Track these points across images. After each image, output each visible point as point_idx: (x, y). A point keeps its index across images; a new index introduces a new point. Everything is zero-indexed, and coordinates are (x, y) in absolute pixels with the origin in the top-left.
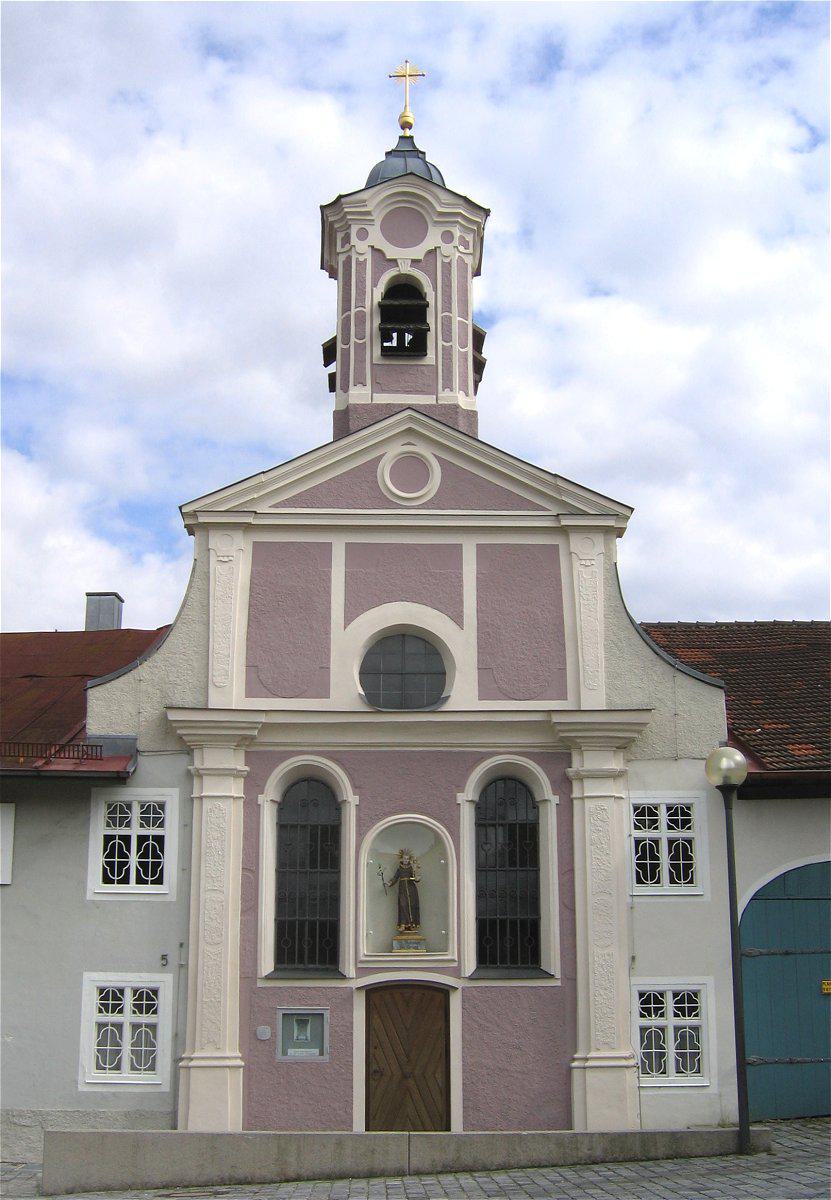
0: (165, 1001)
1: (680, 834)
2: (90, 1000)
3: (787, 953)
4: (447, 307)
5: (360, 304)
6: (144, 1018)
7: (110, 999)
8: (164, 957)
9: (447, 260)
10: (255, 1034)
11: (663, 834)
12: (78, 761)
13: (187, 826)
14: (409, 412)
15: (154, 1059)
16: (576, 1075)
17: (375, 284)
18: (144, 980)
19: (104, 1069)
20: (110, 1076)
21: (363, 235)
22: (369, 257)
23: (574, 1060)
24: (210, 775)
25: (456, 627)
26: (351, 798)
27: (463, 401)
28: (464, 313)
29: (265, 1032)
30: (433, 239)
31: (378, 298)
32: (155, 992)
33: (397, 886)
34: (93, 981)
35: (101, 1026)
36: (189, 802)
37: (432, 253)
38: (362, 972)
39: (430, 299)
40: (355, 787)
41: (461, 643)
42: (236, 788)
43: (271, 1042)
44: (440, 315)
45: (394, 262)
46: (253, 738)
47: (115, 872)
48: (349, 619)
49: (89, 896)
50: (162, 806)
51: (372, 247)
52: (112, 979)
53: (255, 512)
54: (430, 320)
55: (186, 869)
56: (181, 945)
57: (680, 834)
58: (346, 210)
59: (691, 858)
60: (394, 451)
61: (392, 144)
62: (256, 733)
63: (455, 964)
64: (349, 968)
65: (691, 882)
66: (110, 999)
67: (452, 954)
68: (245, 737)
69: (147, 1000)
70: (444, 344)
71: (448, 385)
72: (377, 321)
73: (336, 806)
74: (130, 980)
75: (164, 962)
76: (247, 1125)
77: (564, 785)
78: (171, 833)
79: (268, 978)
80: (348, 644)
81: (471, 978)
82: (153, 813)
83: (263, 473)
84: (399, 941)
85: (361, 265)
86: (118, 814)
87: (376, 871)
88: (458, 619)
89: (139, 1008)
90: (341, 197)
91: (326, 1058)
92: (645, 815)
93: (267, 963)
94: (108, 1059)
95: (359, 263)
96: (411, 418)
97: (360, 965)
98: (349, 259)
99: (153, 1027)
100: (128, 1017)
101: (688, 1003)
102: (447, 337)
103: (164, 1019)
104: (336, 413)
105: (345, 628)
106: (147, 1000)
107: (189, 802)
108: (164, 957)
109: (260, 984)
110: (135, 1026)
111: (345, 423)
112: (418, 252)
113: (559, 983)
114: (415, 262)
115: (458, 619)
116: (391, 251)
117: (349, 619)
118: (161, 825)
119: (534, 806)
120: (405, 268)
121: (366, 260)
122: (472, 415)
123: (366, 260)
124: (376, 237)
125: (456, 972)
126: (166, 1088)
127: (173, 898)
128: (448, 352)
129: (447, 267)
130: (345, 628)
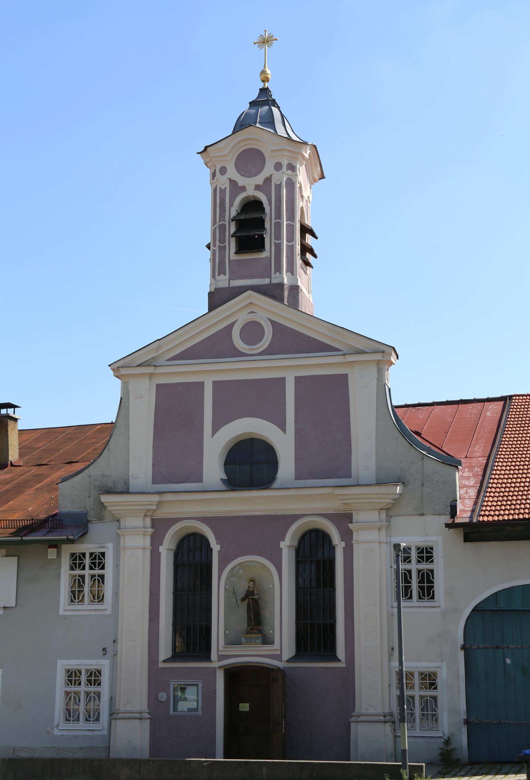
0: (105, 678)
1: (425, 566)
2: (61, 677)
3: (498, 647)
4: (279, 215)
5: (222, 219)
6: (93, 689)
7: (72, 677)
8: (104, 649)
9: (278, 183)
10: (157, 698)
11: (414, 567)
12: (49, 530)
13: (117, 566)
14: (249, 292)
15: (99, 713)
16: (353, 726)
17: (231, 205)
18: (92, 664)
19: (70, 720)
20: (72, 726)
21: (223, 171)
22: (227, 185)
23: (353, 716)
24: (128, 535)
25: (282, 432)
26: (215, 547)
27: (286, 280)
28: (291, 217)
29: (162, 697)
30: (268, 170)
31: (234, 213)
32: (100, 672)
33: (246, 602)
34: (62, 665)
35: (67, 693)
36: (117, 553)
37: (268, 180)
38: (221, 658)
39: (267, 210)
40: (218, 539)
41: (284, 445)
42: (148, 541)
43: (167, 702)
44: (273, 221)
45: (243, 189)
46: (154, 510)
47: (76, 596)
48: (215, 431)
49: (61, 612)
50: (103, 554)
51: (230, 179)
52: (73, 664)
53: (155, 366)
54: (267, 225)
55: (116, 594)
56: (114, 642)
57: (425, 566)
58: (211, 155)
59: (432, 582)
60: (242, 319)
61: (254, 95)
62: (154, 507)
63: (279, 653)
64: (214, 656)
65: (433, 598)
66: (72, 677)
67: (277, 645)
68: (148, 510)
69: (94, 678)
70: (280, 239)
71: (279, 269)
72: (233, 229)
73: (210, 551)
74: (85, 664)
75: (104, 652)
76: (150, 756)
77: (347, 536)
78: (109, 572)
79: (164, 661)
80: (214, 446)
81: (287, 661)
82: (98, 561)
83: (159, 340)
84: (246, 638)
85: (223, 191)
86: (77, 561)
87: (231, 592)
88: (283, 427)
89: (89, 681)
90: (206, 148)
91: (200, 713)
92: (402, 554)
93: (165, 650)
94: (70, 715)
95: (223, 191)
96: (250, 296)
97: (220, 654)
98: (216, 186)
99: (99, 694)
100: (83, 689)
101: (430, 680)
102: (278, 236)
103: (105, 689)
104: (210, 294)
105: (212, 436)
106: (94, 678)
107: (117, 553)
108: (104, 649)
109: (161, 665)
110: (87, 694)
111: (217, 299)
112: (259, 180)
113: (343, 665)
114: (257, 187)
115: (283, 427)
116: (241, 181)
117: (215, 431)
118: (103, 568)
119: (332, 549)
120: (251, 192)
121: (226, 188)
122: (295, 289)
123: (226, 188)
124: (232, 173)
125: (279, 657)
126: (105, 732)
127: (109, 612)
128: (279, 247)
129: (279, 188)
130: (212, 436)
